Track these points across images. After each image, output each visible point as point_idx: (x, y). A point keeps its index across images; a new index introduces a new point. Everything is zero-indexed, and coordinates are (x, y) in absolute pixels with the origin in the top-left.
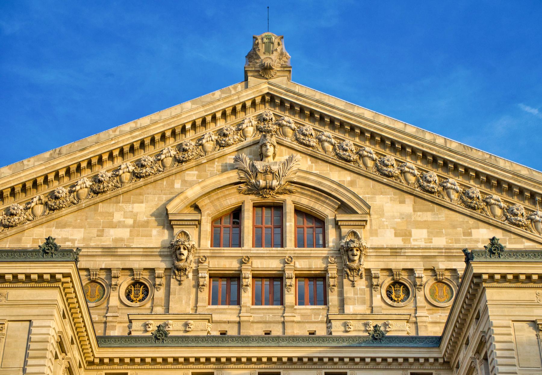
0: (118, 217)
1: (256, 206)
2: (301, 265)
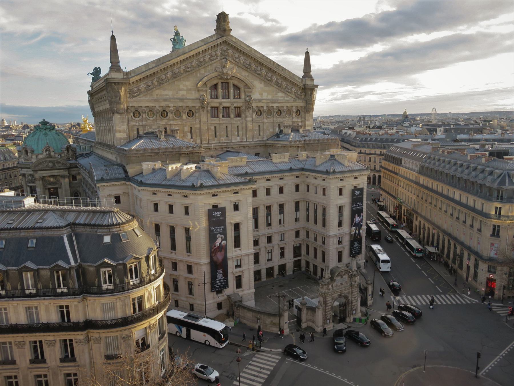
0: (182, 87)
1: (222, 83)
2: (235, 105)
